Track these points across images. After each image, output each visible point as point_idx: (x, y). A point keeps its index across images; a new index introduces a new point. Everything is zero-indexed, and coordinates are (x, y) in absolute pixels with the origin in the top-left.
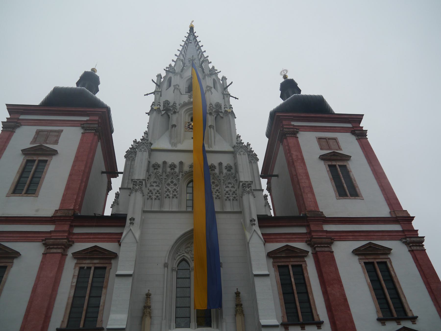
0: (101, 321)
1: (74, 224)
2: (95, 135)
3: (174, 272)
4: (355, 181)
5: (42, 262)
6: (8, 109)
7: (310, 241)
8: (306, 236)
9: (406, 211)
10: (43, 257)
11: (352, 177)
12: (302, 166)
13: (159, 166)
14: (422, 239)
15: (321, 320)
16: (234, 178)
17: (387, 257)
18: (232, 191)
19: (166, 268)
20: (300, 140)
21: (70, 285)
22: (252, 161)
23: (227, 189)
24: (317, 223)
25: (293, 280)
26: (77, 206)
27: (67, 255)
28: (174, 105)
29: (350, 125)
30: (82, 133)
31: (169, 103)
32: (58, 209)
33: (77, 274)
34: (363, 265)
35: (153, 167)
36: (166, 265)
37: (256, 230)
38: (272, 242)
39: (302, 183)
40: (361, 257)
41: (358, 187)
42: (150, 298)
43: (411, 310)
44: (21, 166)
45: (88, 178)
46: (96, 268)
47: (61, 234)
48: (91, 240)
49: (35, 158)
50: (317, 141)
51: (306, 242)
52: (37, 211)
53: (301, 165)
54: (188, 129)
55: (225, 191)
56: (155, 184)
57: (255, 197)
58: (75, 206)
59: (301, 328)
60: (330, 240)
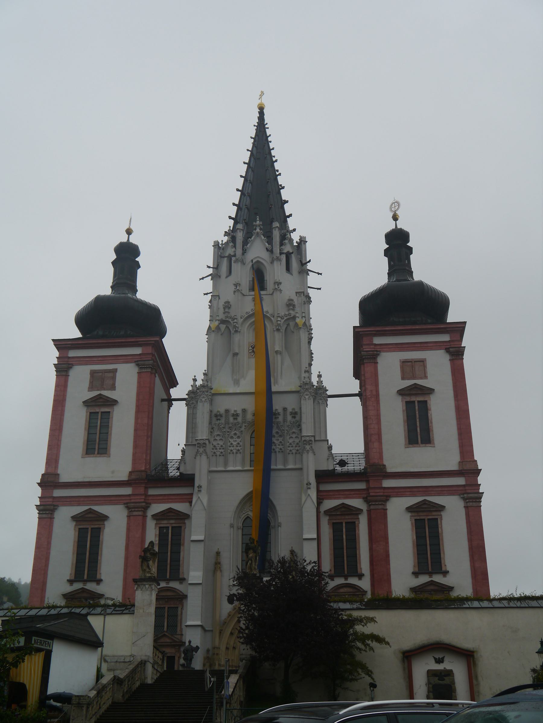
0: (183, 573)
2: (151, 373)
3: (239, 530)
4: (432, 423)
7: (366, 498)
8: (365, 492)
9: (476, 461)
10: (128, 519)
11: (430, 418)
12: (374, 406)
13: (221, 416)
14: (480, 495)
15: (363, 572)
16: (299, 427)
17: (439, 514)
18: (296, 443)
19: (232, 529)
22: (320, 401)
23: (291, 441)
25: (344, 537)
26: (148, 465)
27: (147, 516)
28: (235, 322)
29: (445, 338)
31: (229, 306)
32: (130, 470)
33: (158, 533)
34: (414, 521)
35: (215, 417)
36: (232, 526)
39: (371, 429)
40: (413, 514)
41: (433, 431)
42: (219, 555)
43: (445, 565)
44: (86, 421)
46: (172, 527)
47: (138, 497)
50: (400, 366)
51: (363, 498)
52: (113, 472)
53: (374, 405)
54: (252, 355)
55: (288, 443)
56: (218, 438)
59: (345, 579)
60: (385, 498)
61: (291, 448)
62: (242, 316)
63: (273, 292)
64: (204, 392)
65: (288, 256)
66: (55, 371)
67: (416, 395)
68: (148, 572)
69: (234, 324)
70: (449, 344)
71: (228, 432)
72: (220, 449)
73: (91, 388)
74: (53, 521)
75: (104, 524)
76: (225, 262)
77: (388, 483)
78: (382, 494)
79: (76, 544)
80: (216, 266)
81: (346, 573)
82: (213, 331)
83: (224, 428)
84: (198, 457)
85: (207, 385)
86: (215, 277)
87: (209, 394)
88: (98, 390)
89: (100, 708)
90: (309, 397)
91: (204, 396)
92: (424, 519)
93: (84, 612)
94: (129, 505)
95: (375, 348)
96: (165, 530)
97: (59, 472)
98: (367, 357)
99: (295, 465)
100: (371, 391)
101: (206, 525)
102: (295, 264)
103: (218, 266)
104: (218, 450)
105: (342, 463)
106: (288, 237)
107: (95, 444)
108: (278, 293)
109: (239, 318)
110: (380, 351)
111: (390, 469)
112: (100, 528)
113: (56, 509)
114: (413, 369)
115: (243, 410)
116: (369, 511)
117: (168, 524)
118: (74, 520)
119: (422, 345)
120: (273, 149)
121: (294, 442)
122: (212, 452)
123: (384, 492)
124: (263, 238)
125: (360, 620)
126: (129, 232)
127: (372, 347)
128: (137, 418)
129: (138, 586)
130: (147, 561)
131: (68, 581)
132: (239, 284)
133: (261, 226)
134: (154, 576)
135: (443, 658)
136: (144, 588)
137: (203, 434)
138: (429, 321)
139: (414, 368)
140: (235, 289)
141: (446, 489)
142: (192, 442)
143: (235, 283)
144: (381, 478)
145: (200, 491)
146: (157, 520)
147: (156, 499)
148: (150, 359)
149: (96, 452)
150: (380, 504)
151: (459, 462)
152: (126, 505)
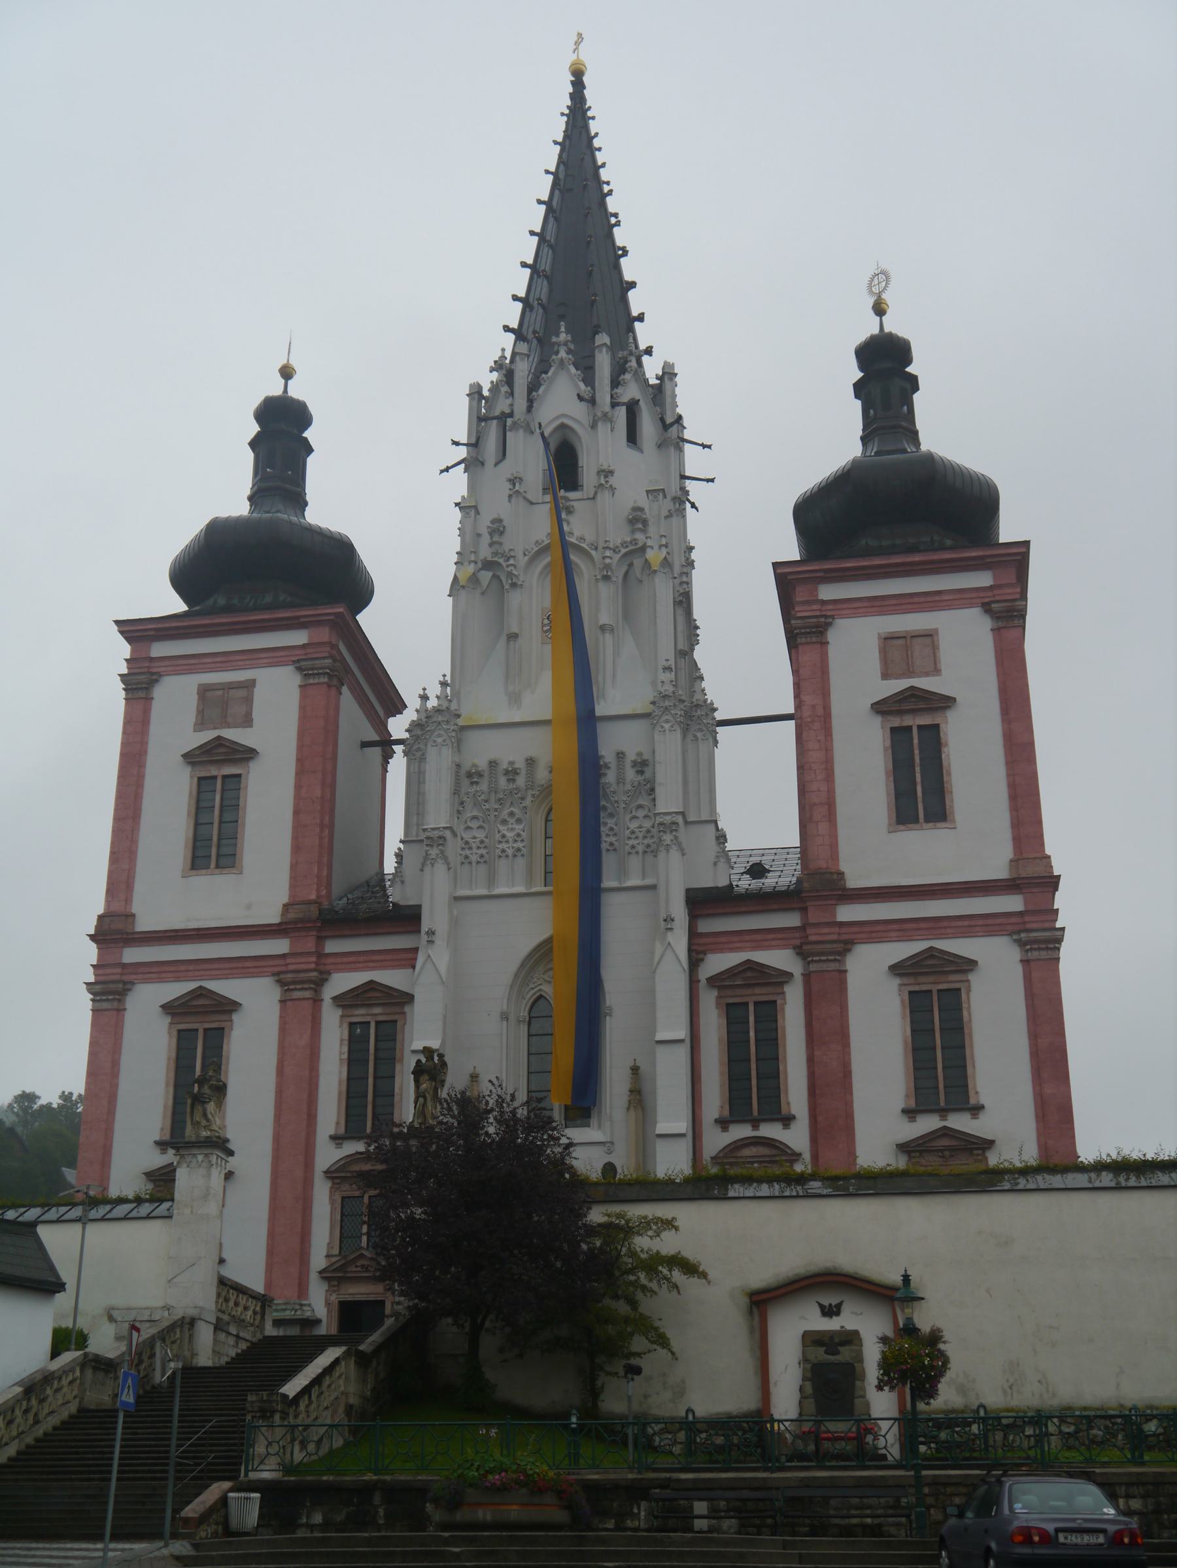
1: (324, 934)
2: (329, 686)
4: (949, 774)
5: (281, 1017)
6: (121, 632)
7: (800, 947)
8: (797, 935)
11: (945, 763)
12: (819, 741)
13: (480, 775)
14: (1058, 933)
15: (793, 1112)
16: (651, 795)
17: (964, 979)
18: (644, 829)
19: (505, 1022)
20: (832, 650)
21: (338, 1058)
22: (699, 735)
23: (633, 825)
24: (824, 903)
25: (752, 1034)
27: (322, 1000)
29: (982, 579)
30: (300, 686)
31: (501, 529)
32: (286, 900)
33: (346, 1036)
35: (468, 777)
36: (505, 1017)
37: (672, 943)
38: (722, 951)
40: (906, 980)
41: (952, 792)
43: (977, 1093)
45: (332, 809)
46: (377, 1023)
47: (303, 960)
48: (361, 965)
49: (213, 771)
51: (794, 948)
52: (249, 907)
53: (819, 738)
56: (474, 824)
57: (683, 855)
58: (318, 890)
60: (843, 945)
61: (635, 842)
62: (527, 550)
63: (596, 493)
64: (439, 723)
65: (632, 409)
66: (124, 689)
67: (913, 712)
68: (205, 1127)
69: (509, 569)
70: (990, 594)
71: (496, 810)
72: (479, 848)
73: (201, 723)
74: (123, 1016)
75: (231, 1020)
76: (493, 427)
77: (847, 913)
78: (834, 937)
79: (173, 1065)
80: (473, 441)
81: (755, 1113)
82: (463, 587)
83: (486, 801)
84: (428, 869)
85: (448, 708)
86: (473, 464)
87: (452, 728)
88: (215, 728)
89: (37, 1422)
90: (672, 726)
91: (442, 733)
92: (931, 991)
93: (32, 1214)
94: (282, 976)
95: (824, 609)
96: (359, 1030)
97: (133, 911)
98: (803, 631)
99: (644, 877)
100: (814, 707)
101: (445, 1017)
102: (648, 427)
103: (478, 439)
104: (475, 850)
105: (757, 871)
106: (630, 367)
107: (210, 847)
108: (607, 494)
109: (520, 556)
110: (833, 617)
111: (854, 882)
112: (223, 1029)
113: (130, 990)
114: (907, 653)
115: (527, 760)
116: (807, 977)
117: (368, 1015)
118: (168, 1014)
119: (929, 599)
120: (603, 165)
121: (640, 827)
122: (461, 855)
123: (839, 934)
124: (573, 369)
125: (646, 1224)
126: (287, 373)
127: (815, 607)
128: (298, 787)
129: (181, 1158)
130: (204, 1103)
131: (157, 1143)
132: (519, 478)
133: (569, 344)
134: (217, 1134)
135: (839, 1306)
136: (194, 1160)
137: (438, 816)
138: (948, 542)
139: (909, 652)
140: (510, 489)
141: (980, 922)
142: (417, 835)
143: (510, 476)
144: (834, 902)
145: (431, 942)
146: (343, 1007)
147: (342, 963)
148: (326, 655)
149: (213, 865)
150: (831, 961)
151: (1011, 861)
152: (276, 978)
